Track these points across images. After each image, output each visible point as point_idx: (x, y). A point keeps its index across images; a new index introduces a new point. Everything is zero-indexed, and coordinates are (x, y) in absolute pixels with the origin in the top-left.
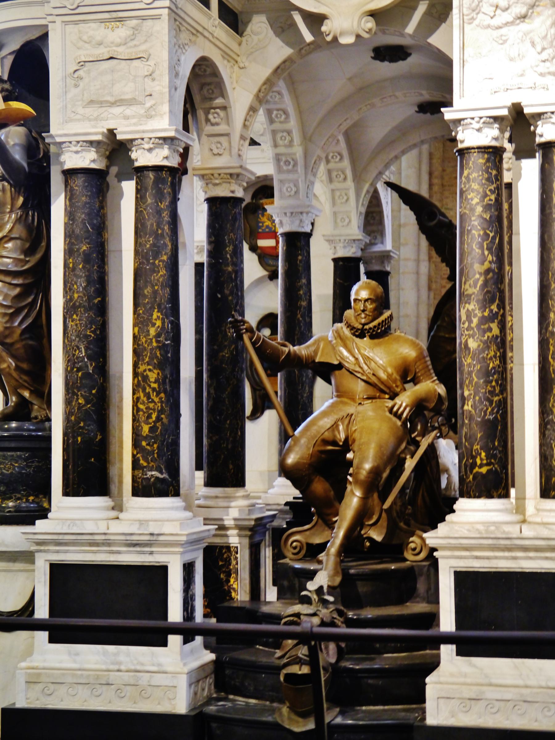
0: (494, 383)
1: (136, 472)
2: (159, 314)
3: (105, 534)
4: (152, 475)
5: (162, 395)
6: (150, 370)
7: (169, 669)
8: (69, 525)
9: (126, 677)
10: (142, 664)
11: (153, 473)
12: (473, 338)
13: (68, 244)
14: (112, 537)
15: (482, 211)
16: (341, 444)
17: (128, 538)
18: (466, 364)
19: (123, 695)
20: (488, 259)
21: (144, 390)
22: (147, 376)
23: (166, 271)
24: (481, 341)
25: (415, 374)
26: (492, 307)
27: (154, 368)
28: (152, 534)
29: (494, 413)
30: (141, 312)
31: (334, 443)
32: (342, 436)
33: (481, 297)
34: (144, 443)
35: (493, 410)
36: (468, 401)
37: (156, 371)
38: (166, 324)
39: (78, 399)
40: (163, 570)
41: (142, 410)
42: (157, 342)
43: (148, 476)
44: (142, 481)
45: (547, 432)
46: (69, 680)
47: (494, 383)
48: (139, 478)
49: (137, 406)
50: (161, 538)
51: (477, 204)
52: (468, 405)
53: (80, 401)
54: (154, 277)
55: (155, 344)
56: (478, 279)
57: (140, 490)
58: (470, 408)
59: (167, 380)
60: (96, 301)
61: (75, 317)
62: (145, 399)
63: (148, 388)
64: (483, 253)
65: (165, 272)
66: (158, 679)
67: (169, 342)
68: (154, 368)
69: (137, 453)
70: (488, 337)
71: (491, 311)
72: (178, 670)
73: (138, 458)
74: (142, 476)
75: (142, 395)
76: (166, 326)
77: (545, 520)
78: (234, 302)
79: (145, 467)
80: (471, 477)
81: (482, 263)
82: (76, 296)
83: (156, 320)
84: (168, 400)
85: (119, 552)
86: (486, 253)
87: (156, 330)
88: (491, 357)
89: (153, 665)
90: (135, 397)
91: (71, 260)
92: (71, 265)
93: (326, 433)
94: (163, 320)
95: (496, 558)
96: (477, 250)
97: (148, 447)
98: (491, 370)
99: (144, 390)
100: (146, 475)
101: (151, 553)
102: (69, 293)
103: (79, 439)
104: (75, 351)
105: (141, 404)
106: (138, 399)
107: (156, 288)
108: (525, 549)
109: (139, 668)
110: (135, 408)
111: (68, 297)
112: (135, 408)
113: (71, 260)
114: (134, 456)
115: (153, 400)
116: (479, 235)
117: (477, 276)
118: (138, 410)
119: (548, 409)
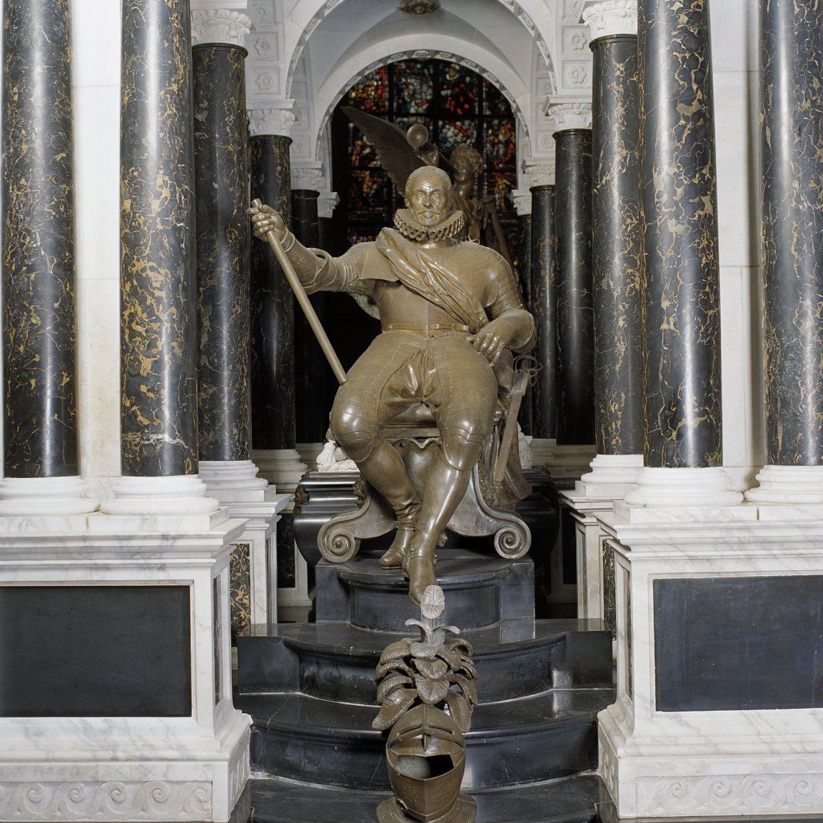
0: (707, 289)
1: (130, 436)
2: (167, 178)
3: (84, 538)
4: (158, 440)
6: (152, 269)
7: (198, 754)
8: (20, 524)
9: (127, 769)
10: (152, 747)
12: (677, 218)
13: (11, 64)
14: (97, 544)
15: (688, 22)
16: (413, 393)
17: (124, 543)
18: (664, 258)
19: (122, 798)
20: (697, 98)
21: (142, 301)
22: (147, 278)
23: (177, 109)
24: (689, 222)
25: (498, 298)
26: (704, 172)
27: (160, 265)
28: (165, 537)
29: (708, 336)
30: (136, 174)
31: (404, 392)
32: (415, 383)
33: (688, 155)
34: (143, 388)
35: (706, 330)
36: (669, 316)
37: (162, 271)
38: (178, 194)
39: (29, 317)
40: (182, 593)
41: (140, 334)
42: (163, 223)
43: (152, 441)
44: (141, 449)
45: (788, 364)
46: (29, 777)
47: (707, 289)
48: (136, 445)
49: (130, 328)
50: (180, 543)
51: (680, 10)
52: (668, 323)
53: (34, 321)
55: (160, 227)
56: (684, 127)
58: (672, 327)
59: (180, 286)
60: (58, 157)
61: (23, 181)
63: (149, 298)
64: (690, 88)
65: (175, 111)
66: (182, 771)
67: (182, 224)
68: (160, 265)
69: (132, 405)
70: (700, 216)
71: (703, 176)
72: (214, 754)
73: (134, 412)
74: (142, 442)
75: (139, 310)
76: (178, 198)
77: (792, 498)
78: (238, 194)
79: (147, 427)
80: (674, 433)
81: (689, 104)
83: (161, 187)
85: (107, 568)
86: (695, 87)
87: (162, 204)
88: (703, 248)
89: (170, 747)
90: (127, 313)
91: (15, 90)
92: (16, 98)
93: (392, 378)
94: (172, 186)
95: (722, 558)
96: (681, 83)
97: (151, 395)
98: (704, 267)
100: (148, 440)
101: (162, 567)
102: (12, 143)
104: (24, 238)
105: (137, 324)
106: (132, 316)
108: (765, 542)
109: (147, 754)
110: (127, 331)
112: (127, 331)
114: (123, 408)
115: (157, 317)
116: (684, 59)
117: (682, 122)
118: (133, 334)
119: (789, 327)
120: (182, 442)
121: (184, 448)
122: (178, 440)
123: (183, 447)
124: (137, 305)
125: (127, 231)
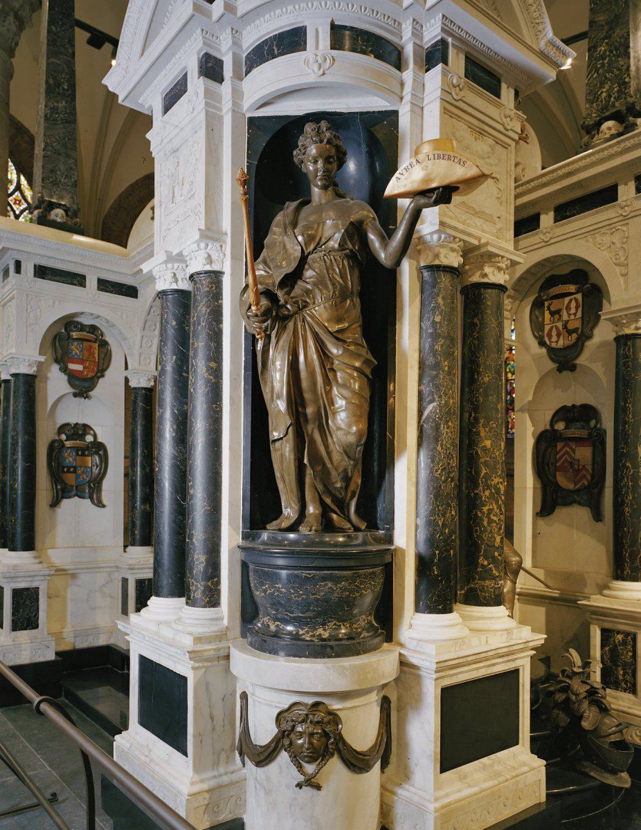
34: (496, 554)
41: (495, 522)
48: (492, 588)
61: (450, 424)
62: (498, 511)
75: (495, 507)
79: (497, 577)
82: (451, 401)
91: (446, 363)
92: (446, 369)
97: (499, 558)
99: (497, 502)
102: (443, 397)
103: (452, 552)
105: (494, 515)
111: (443, 402)
113: (446, 363)
124: (494, 505)
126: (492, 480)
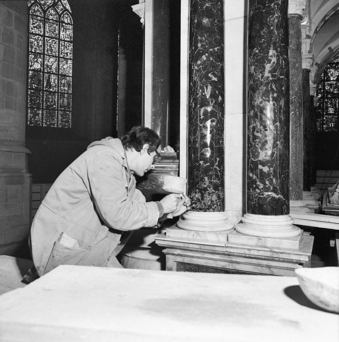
2: (275, 52)
4: (268, 195)
5: (278, 124)
11: (270, 193)
23: (280, 13)
30: (257, 51)
38: (281, 61)
43: (265, 196)
44: (258, 200)
48: (256, 198)
49: (253, 135)
54: (270, 18)
57: (253, 205)
59: (282, 110)
65: (279, 14)
67: (283, 77)
74: (259, 196)
75: (259, 124)
76: (281, 62)
83: (271, 56)
84: (282, 128)
100: (263, 195)
105: (257, 132)
106: (254, 128)
107: (272, 28)
118: (255, 137)
120: (282, 197)
121: (283, 200)
122: (280, 196)
123: (282, 199)
124: (257, 122)
125: (252, 83)
126: (255, 101)
